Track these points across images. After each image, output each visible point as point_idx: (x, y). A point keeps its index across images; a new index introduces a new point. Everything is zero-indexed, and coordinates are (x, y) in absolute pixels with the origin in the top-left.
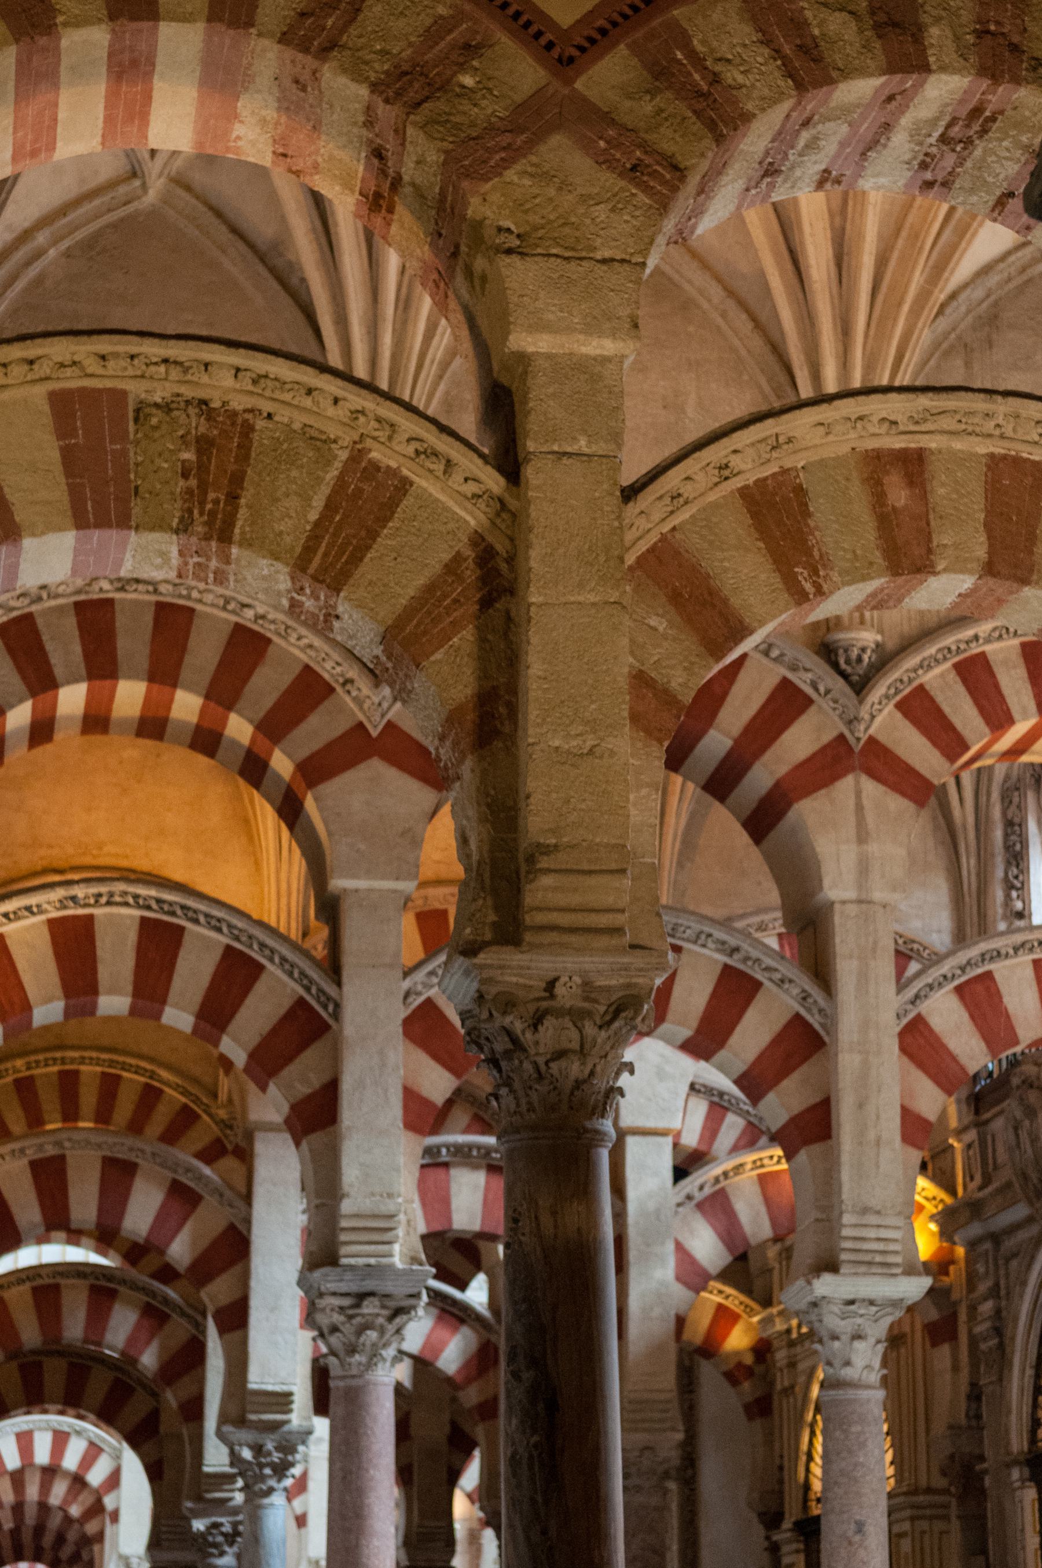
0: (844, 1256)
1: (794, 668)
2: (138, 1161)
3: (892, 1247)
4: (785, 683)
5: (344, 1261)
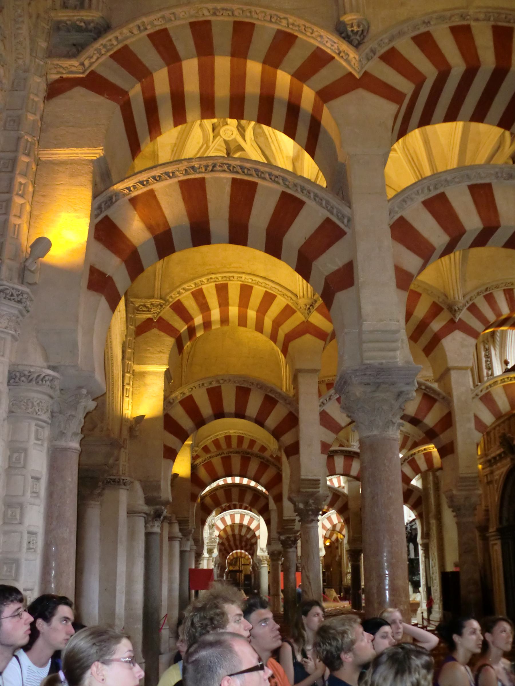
2: (251, 387)
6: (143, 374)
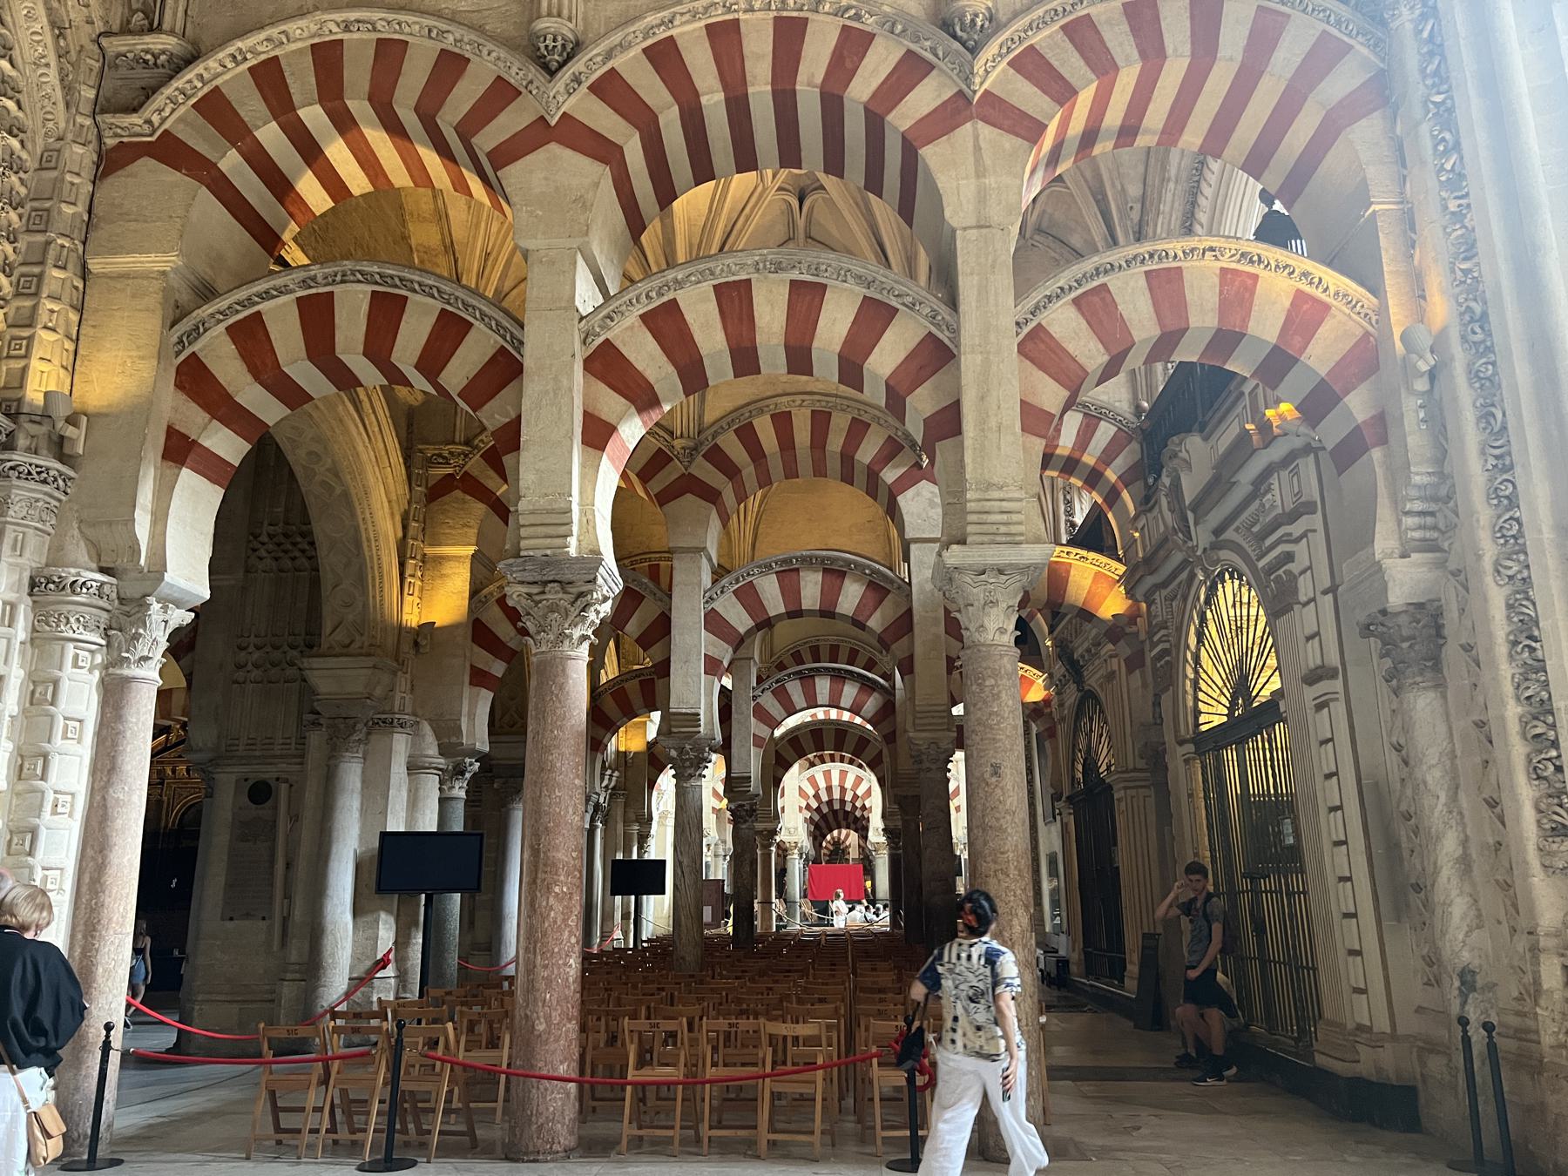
0: (970, 529)
1: (917, 40)
3: (1015, 517)
4: (909, 52)
5: (522, 553)
6: (440, 560)
